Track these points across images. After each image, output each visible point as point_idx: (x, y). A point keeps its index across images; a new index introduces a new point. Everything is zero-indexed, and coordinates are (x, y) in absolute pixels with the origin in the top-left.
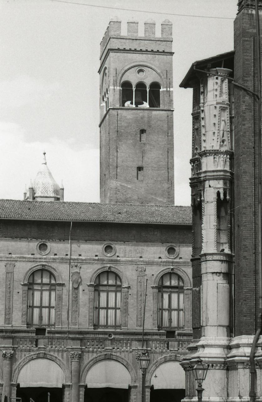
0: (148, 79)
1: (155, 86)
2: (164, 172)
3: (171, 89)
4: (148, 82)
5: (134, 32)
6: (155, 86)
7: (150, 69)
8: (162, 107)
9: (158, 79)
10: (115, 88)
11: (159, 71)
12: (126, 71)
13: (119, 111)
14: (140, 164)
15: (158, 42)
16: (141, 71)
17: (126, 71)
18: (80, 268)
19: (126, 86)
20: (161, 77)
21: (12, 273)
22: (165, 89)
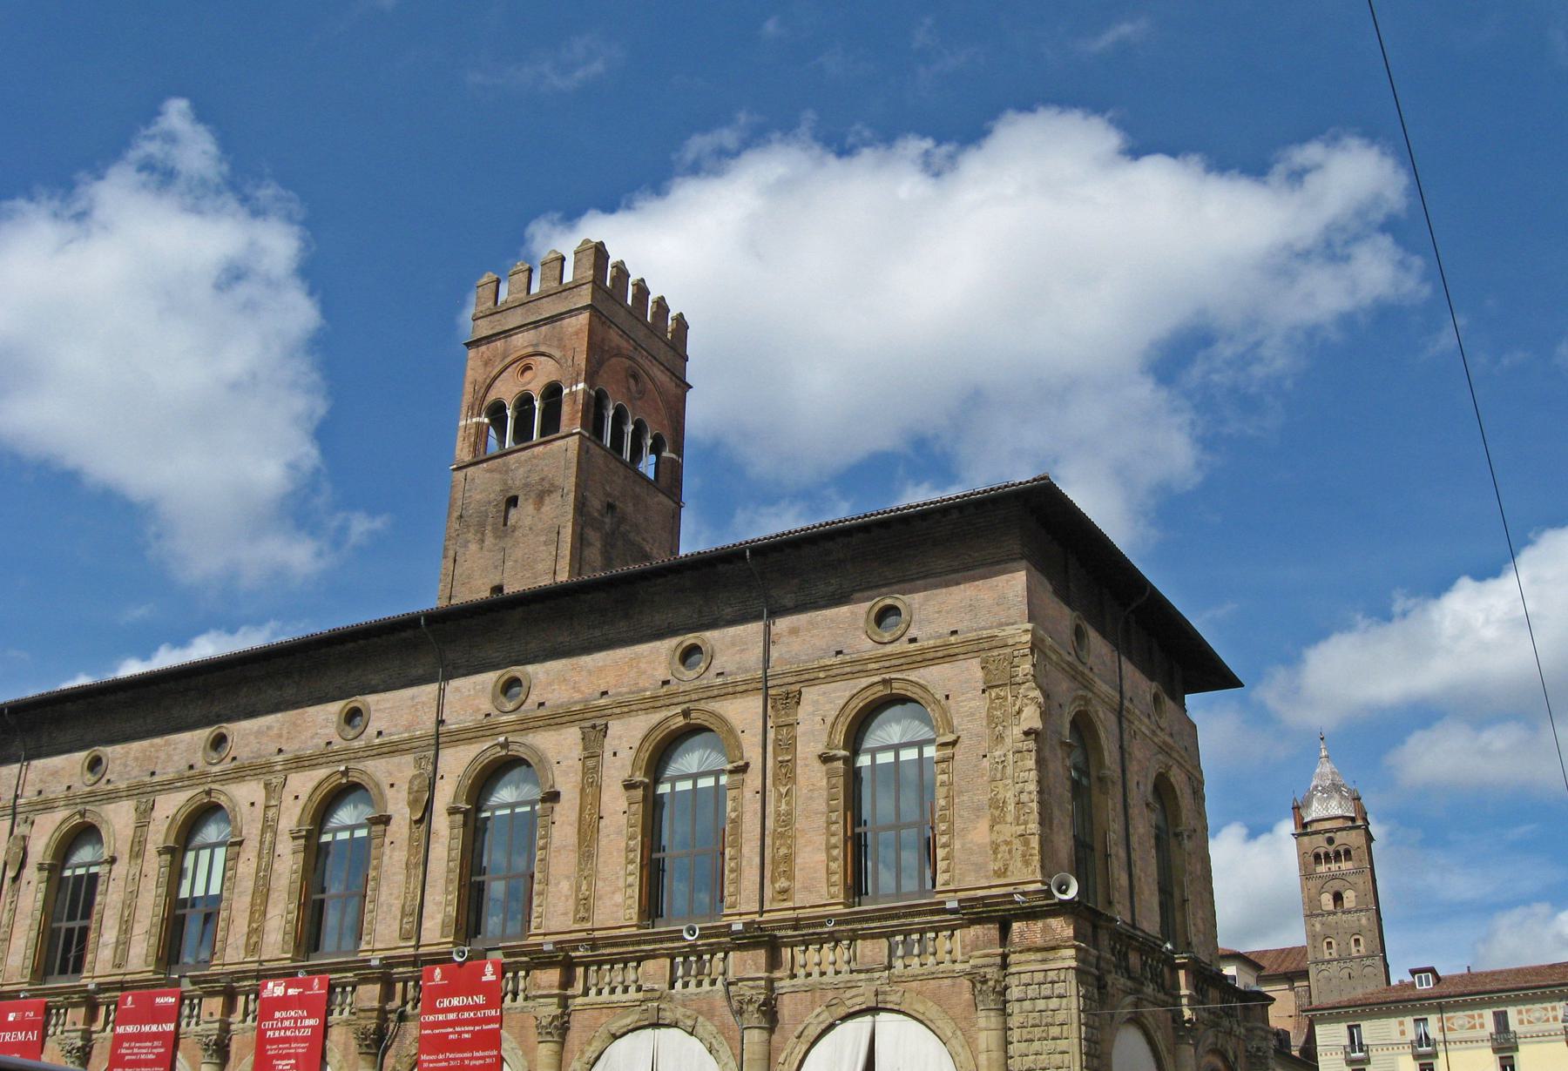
1: (553, 392)
4: (536, 387)
6: (553, 392)
7: (543, 358)
8: (564, 430)
10: (469, 421)
12: (495, 378)
13: (471, 470)
14: (496, 582)
15: (564, 294)
16: (528, 368)
18: (33, 823)
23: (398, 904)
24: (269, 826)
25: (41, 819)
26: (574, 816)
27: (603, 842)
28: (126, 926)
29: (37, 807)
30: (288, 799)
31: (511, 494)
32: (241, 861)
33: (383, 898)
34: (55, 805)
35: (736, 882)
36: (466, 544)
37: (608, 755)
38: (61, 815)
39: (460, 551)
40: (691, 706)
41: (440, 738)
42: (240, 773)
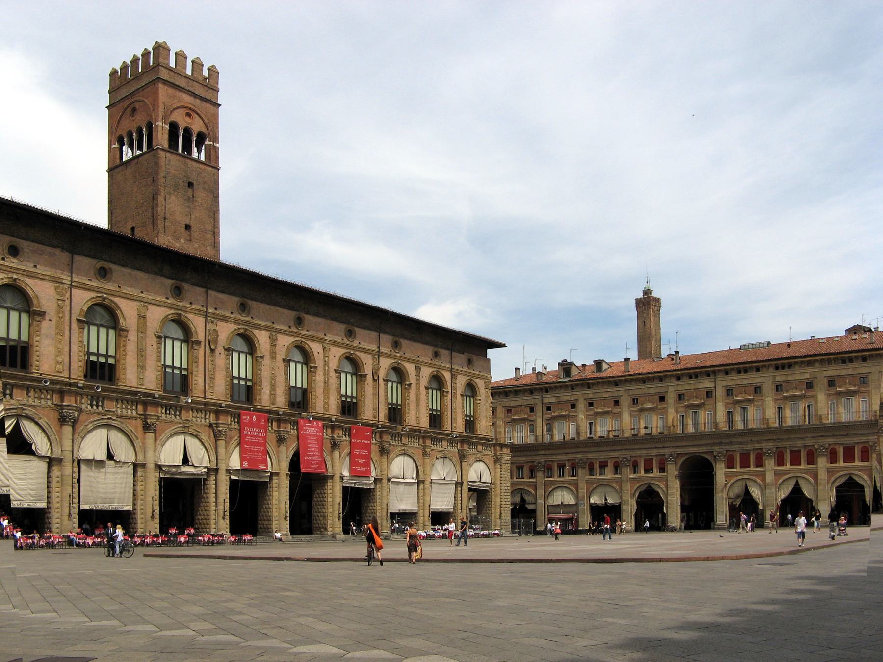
0: (197, 126)
2: (209, 236)
3: (217, 145)
5: (183, 68)
9: (204, 130)
11: (206, 121)
12: (175, 109)
15: (206, 88)
16: (188, 115)
17: (175, 109)
19: (174, 127)
20: (207, 128)
21: (144, 317)
22: (212, 143)
23: (371, 405)
24: (326, 364)
25: (221, 324)
26: (414, 392)
27: (421, 402)
28: (273, 387)
29: (219, 317)
30: (331, 357)
31: (190, 181)
32: (317, 375)
33: (366, 403)
34: (229, 320)
35: (447, 422)
36: (170, 194)
37: (421, 376)
38: (232, 327)
39: (167, 196)
40: (439, 370)
41: (379, 354)
42: (313, 339)
